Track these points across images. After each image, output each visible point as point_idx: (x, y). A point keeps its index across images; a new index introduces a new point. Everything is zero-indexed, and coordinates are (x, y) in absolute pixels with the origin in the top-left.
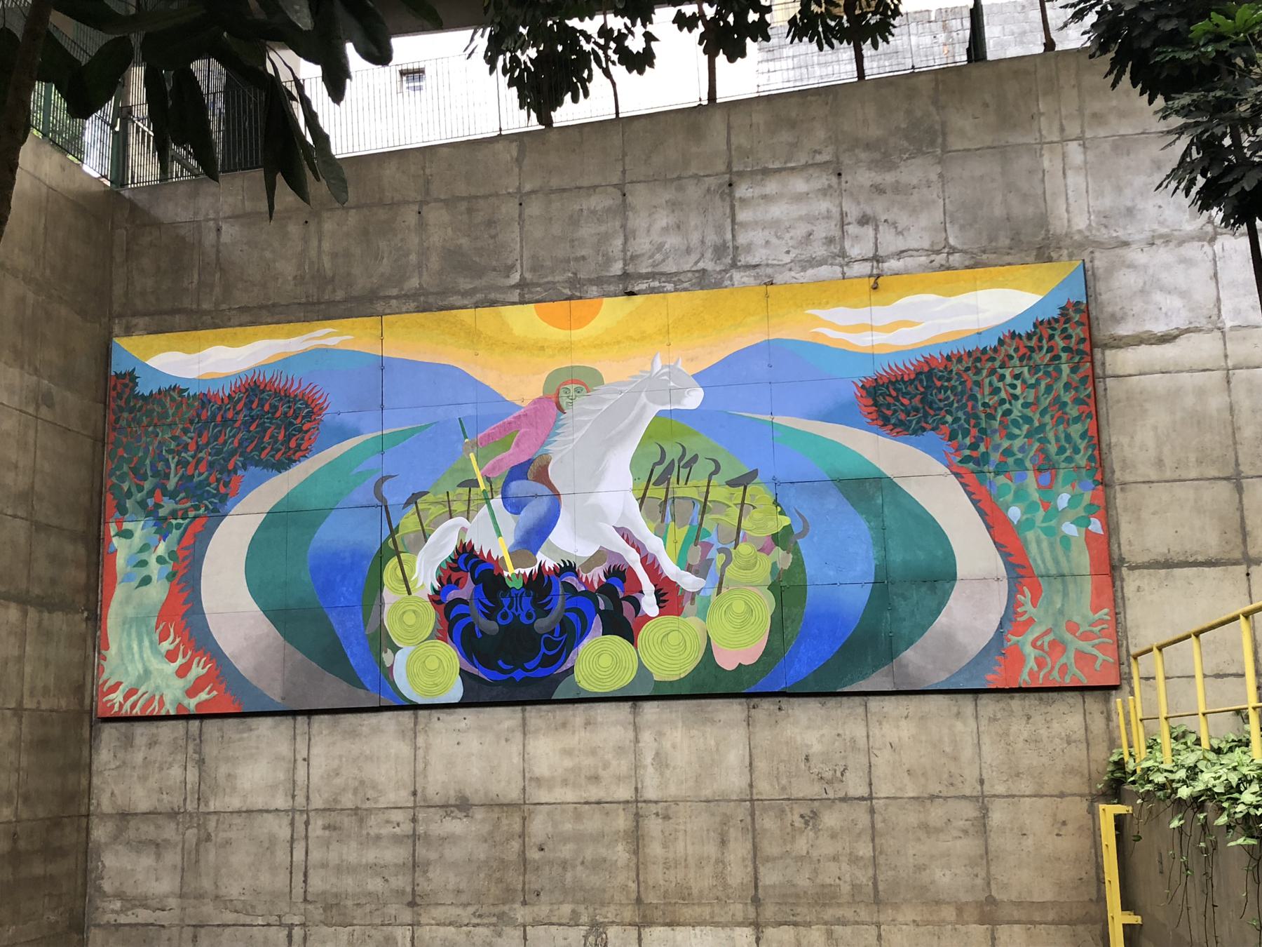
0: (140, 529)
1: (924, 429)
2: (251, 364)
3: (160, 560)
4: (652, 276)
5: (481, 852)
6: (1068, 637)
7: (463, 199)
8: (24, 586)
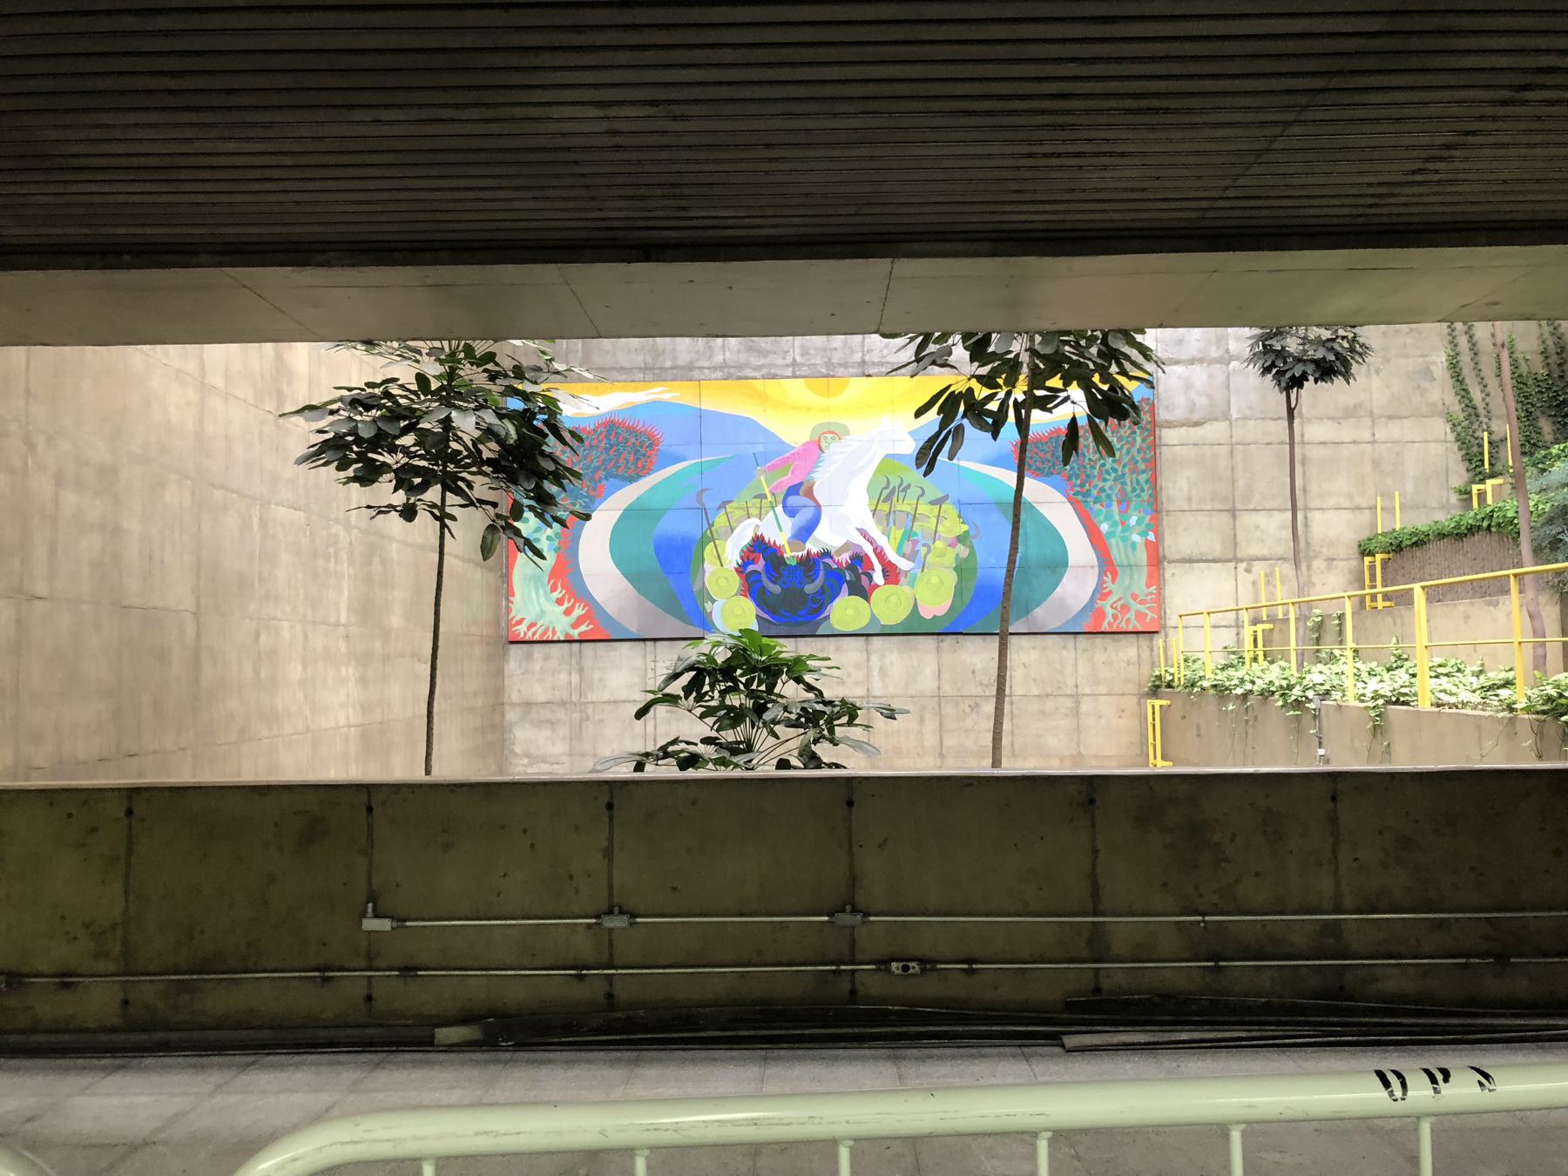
3: (549, 538)
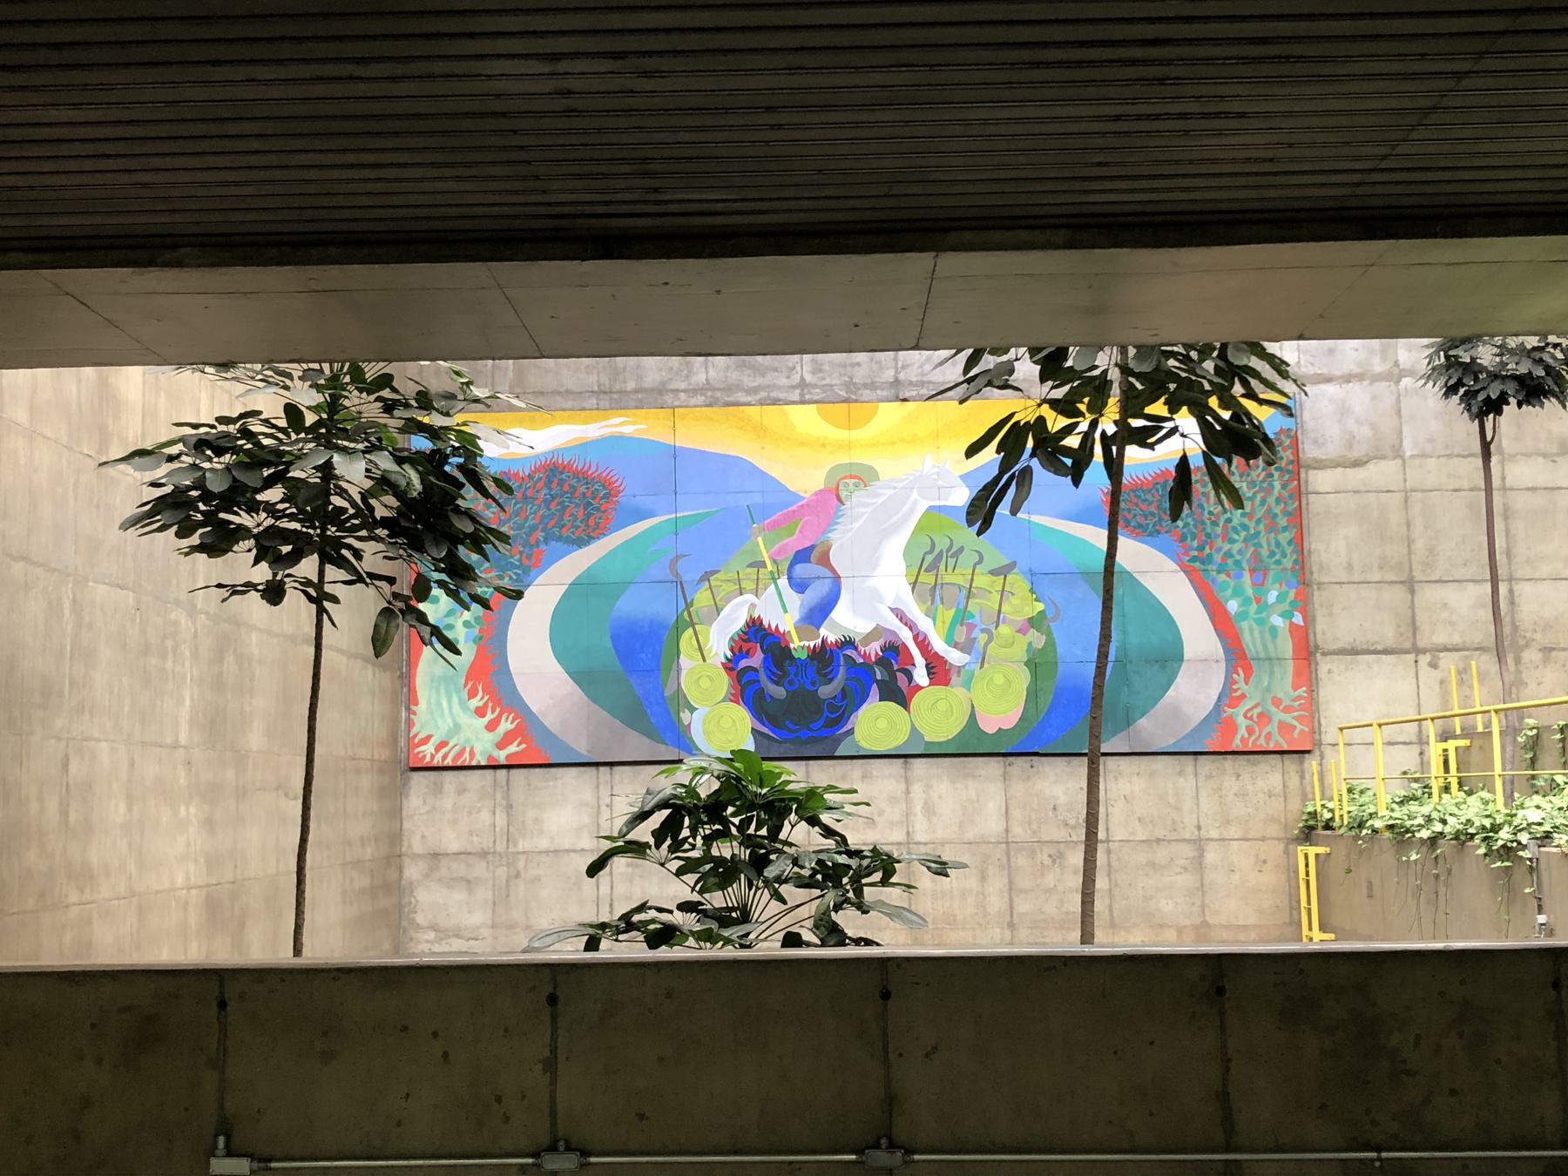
2: (551, 446)
3: (466, 624)
6: (1273, 709)
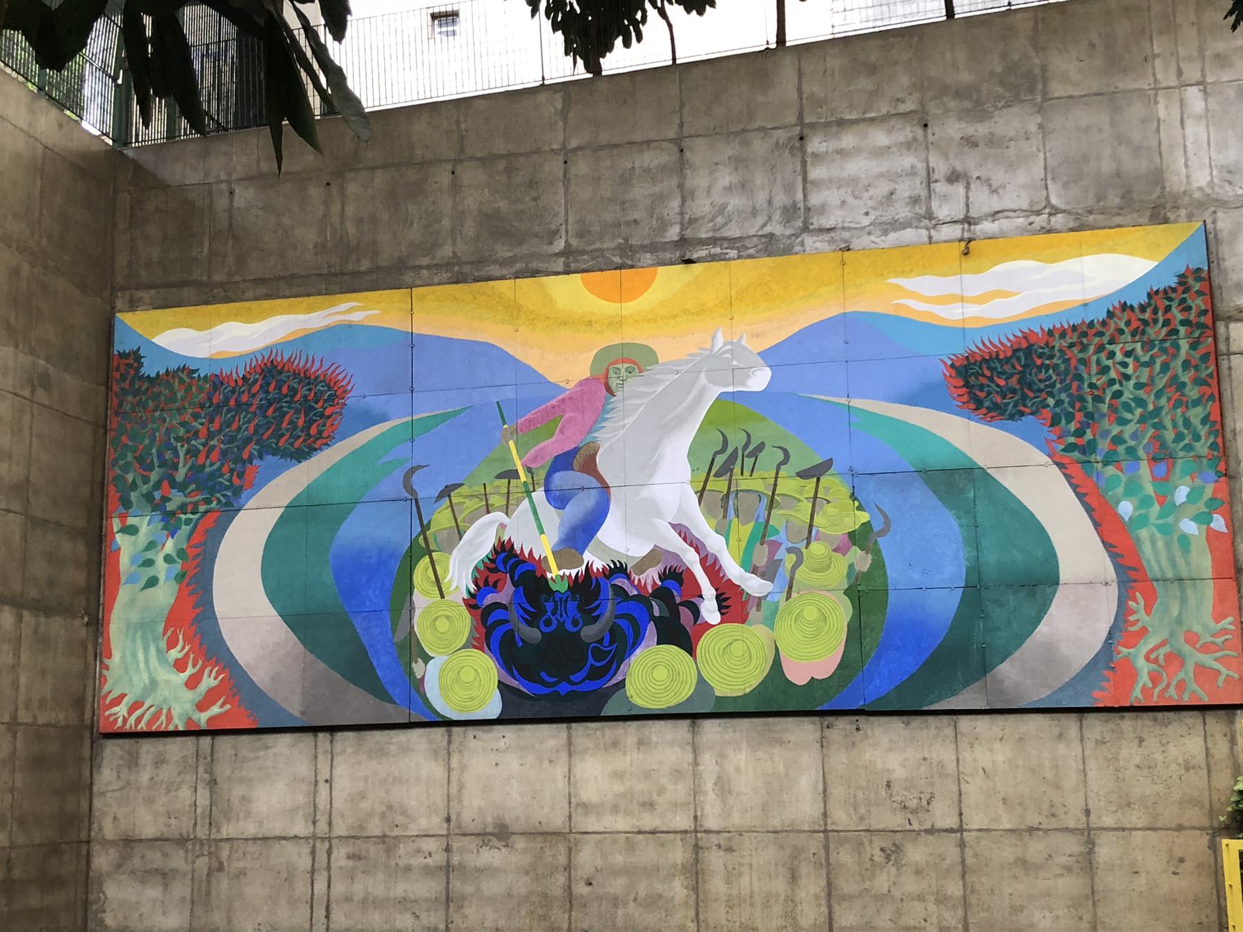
0: (146, 524)
1: (1022, 414)
2: (268, 341)
3: (168, 559)
4: (714, 241)
5: (522, 886)
6: (1187, 648)
7: (502, 157)
8: (17, 587)
